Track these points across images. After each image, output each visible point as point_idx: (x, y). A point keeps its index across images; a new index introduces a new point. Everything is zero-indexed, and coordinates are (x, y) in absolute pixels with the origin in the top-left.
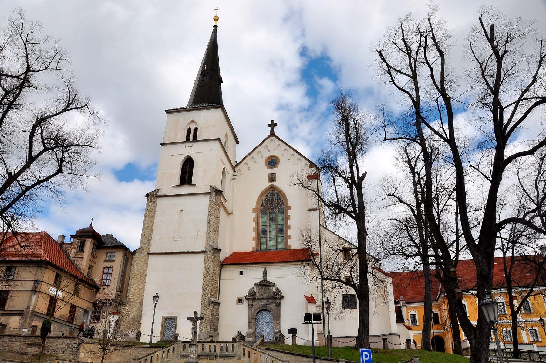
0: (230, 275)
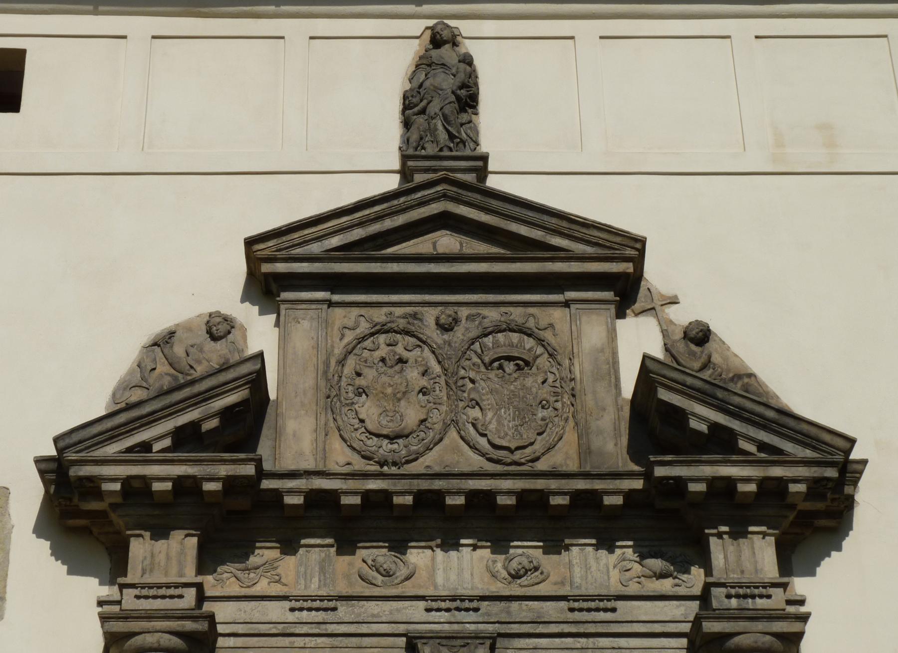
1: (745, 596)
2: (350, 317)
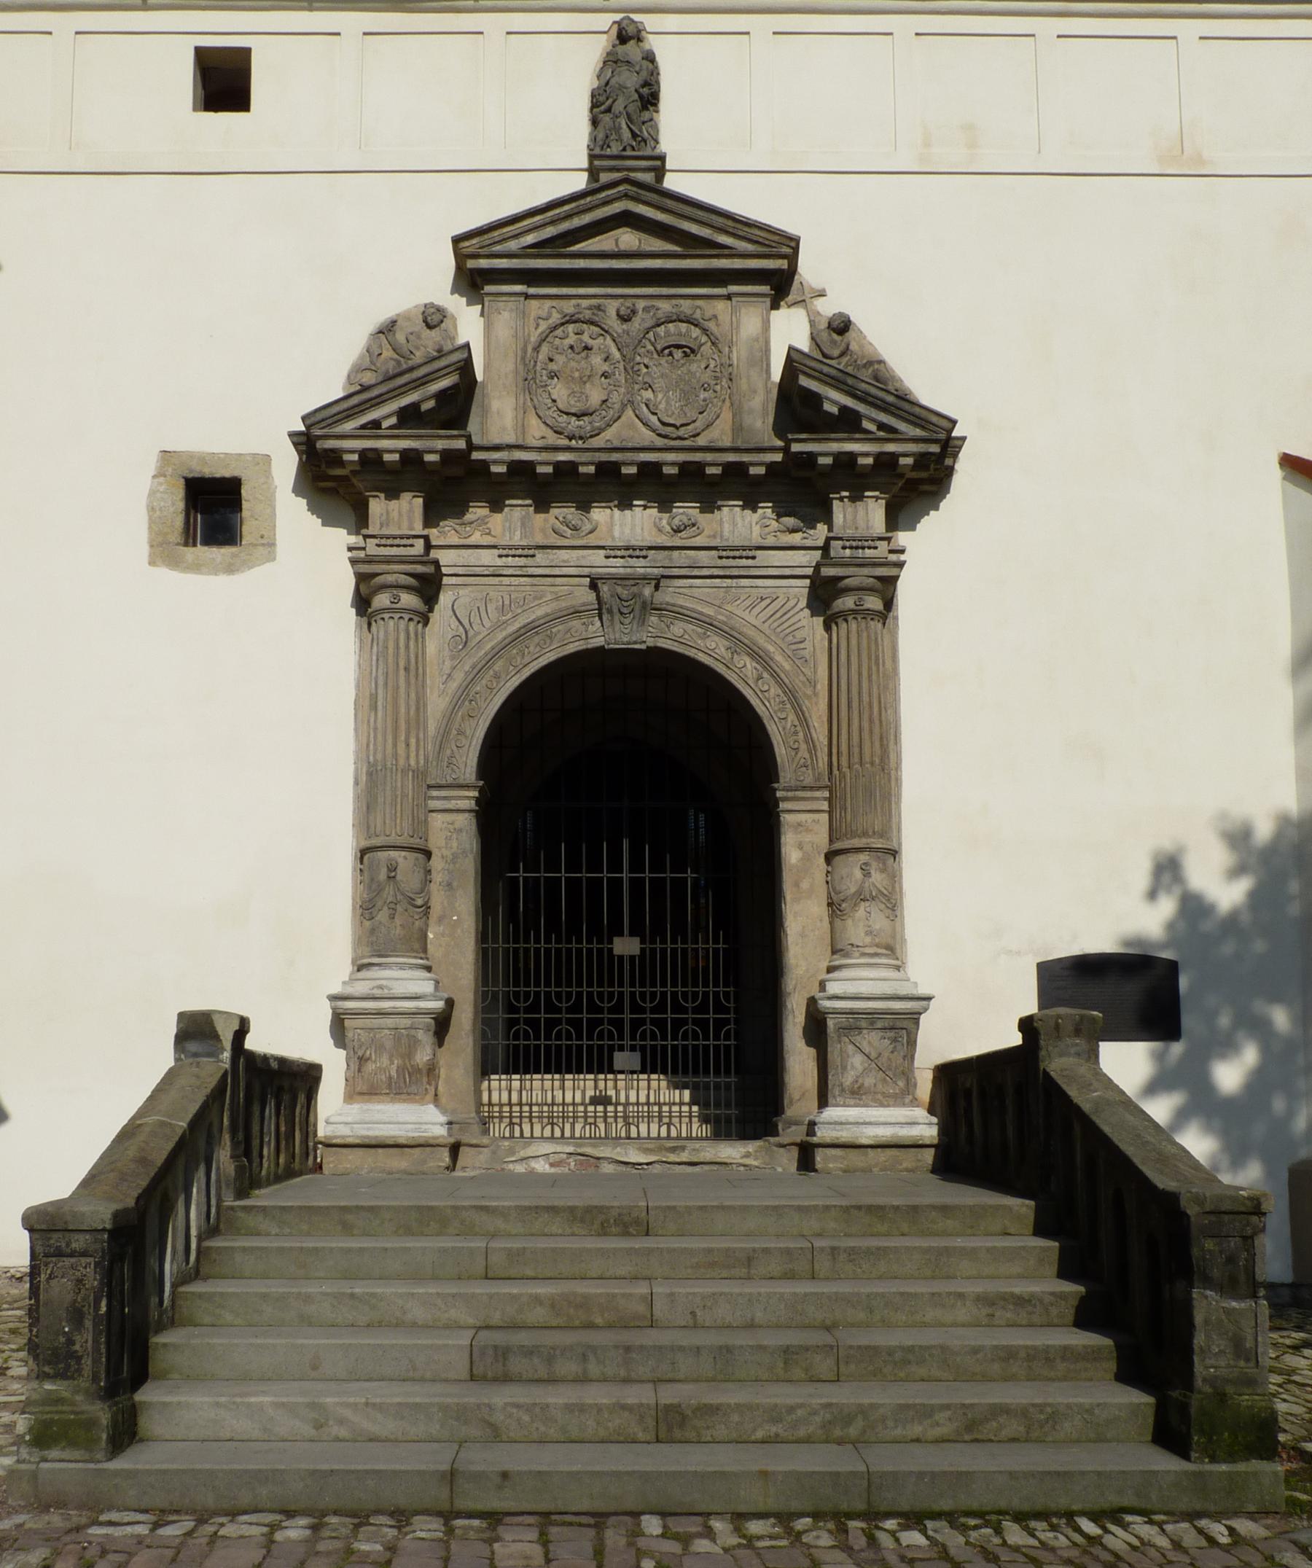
1: (857, 548)
2: (545, 308)
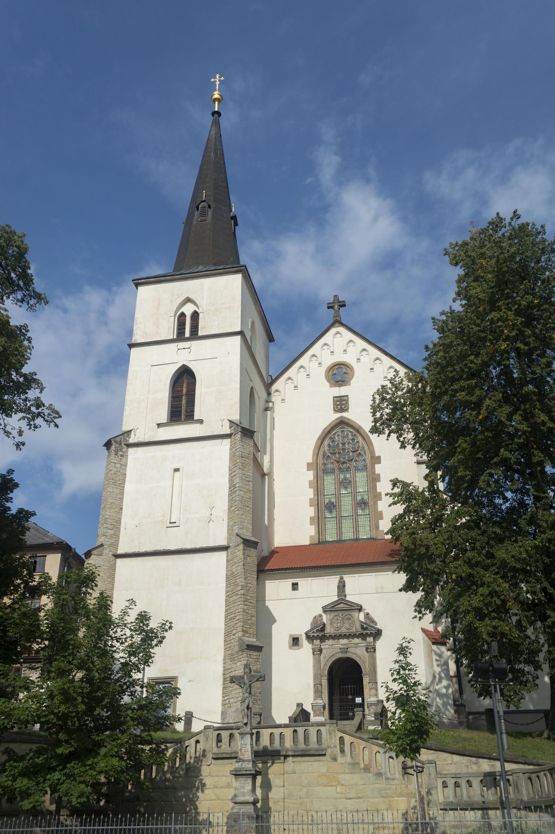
0: (276, 590)
2: (333, 614)
